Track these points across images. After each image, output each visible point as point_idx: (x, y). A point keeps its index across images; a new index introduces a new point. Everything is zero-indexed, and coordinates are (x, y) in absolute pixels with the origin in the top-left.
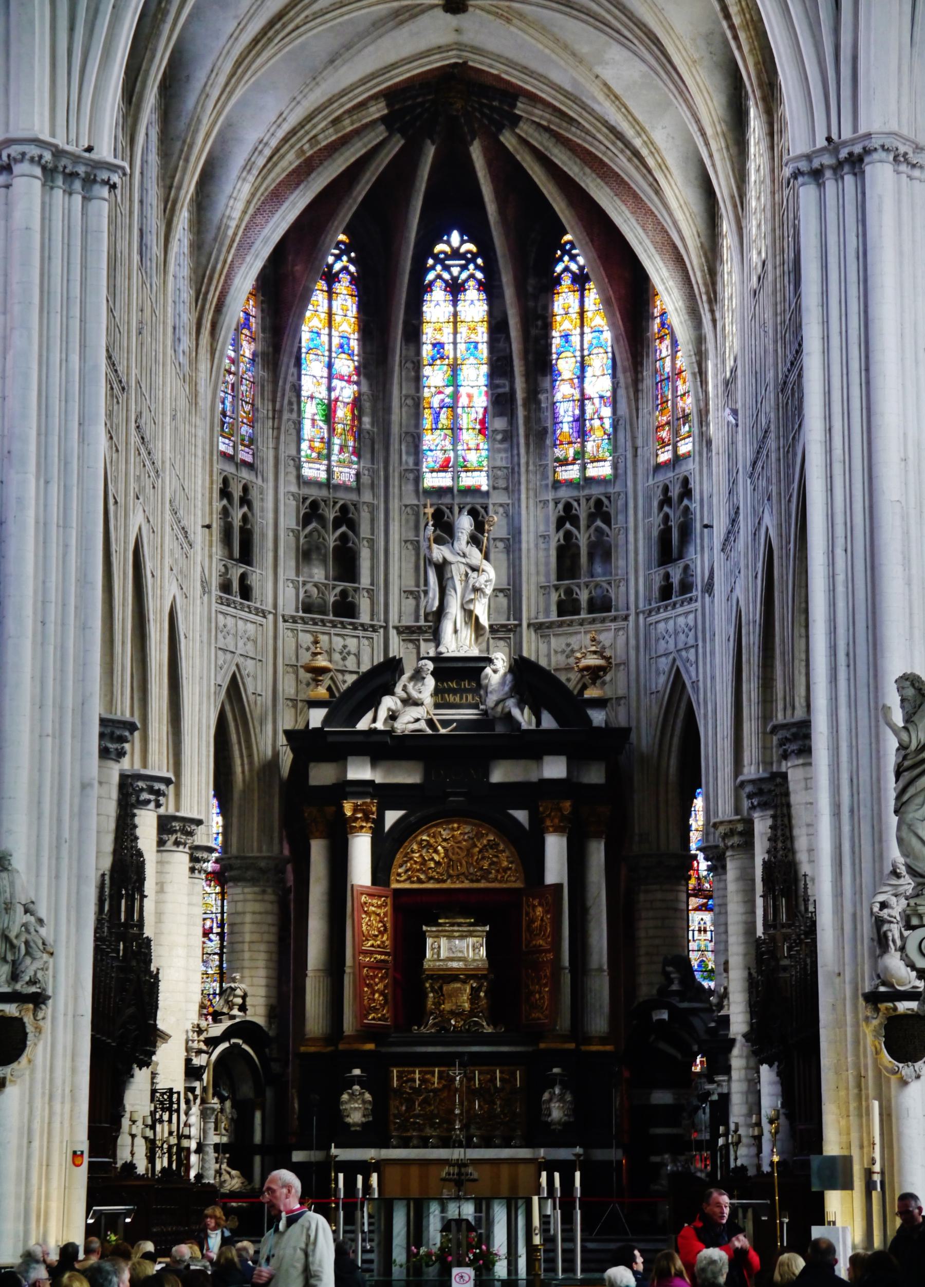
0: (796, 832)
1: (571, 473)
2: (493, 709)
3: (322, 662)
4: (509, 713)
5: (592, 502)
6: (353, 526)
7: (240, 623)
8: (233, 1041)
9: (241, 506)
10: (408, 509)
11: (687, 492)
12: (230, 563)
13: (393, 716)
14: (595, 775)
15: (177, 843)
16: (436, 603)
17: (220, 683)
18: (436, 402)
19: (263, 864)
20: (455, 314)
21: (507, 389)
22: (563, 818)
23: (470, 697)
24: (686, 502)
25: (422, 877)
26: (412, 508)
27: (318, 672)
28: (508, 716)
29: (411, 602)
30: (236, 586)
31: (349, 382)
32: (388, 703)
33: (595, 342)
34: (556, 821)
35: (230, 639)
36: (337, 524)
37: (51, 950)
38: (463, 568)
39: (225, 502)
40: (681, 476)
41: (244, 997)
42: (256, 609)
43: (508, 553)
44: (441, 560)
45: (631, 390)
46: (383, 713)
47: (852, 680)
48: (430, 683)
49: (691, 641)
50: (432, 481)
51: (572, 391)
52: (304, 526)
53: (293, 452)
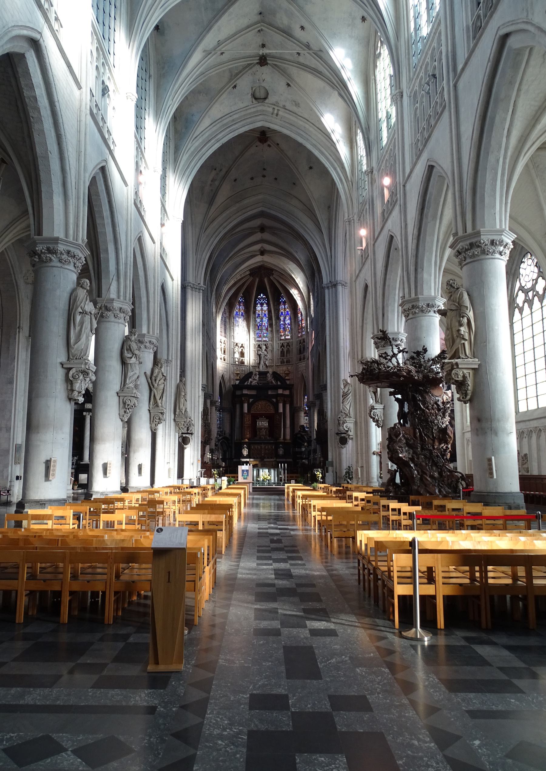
1: (283, 338)
6: (243, 347)
11: (304, 342)
14: (287, 392)
27: (238, 374)
28: (272, 382)
32: (250, 380)
36: (241, 347)
47: (334, 378)
48: (258, 376)
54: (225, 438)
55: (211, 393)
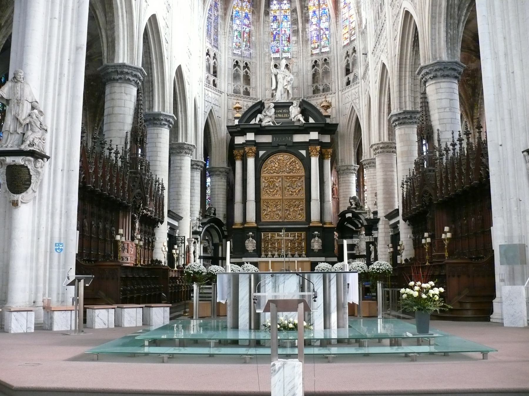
0: (432, 113)
2: (294, 118)
3: (238, 105)
4: (299, 119)
5: (323, 60)
7: (213, 94)
8: (211, 224)
9: (213, 59)
12: (210, 75)
13: (261, 120)
14: (327, 139)
15: (186, 153)
17: (206, 111)
18: (274, 33)
19: (221, 170)
20: (281, 7)
21: (296, 29)
22: (317, 151)
23: (286, 115)
24: (354, 54)
25: (272, 172)
28: (299, 120)
30: (212, 82)
31: (248, 27)
32: (259, 116)
33: (323, 12)
34: (315, 153)
35: (209, 98)
37: (45, 128)
38: (283, 75)
39: (208, 56)
40: (352, 47)
41: (215, 211)
42: (218, 90)
44: (276, 73)
45: (335, 24)
46: (258, 119)
49: (357, 97)
50: (273, 56)
51: (316, 27)
52: (234, 68)
53: (231, 46)
54: (217, 221)
55: (172, 114)
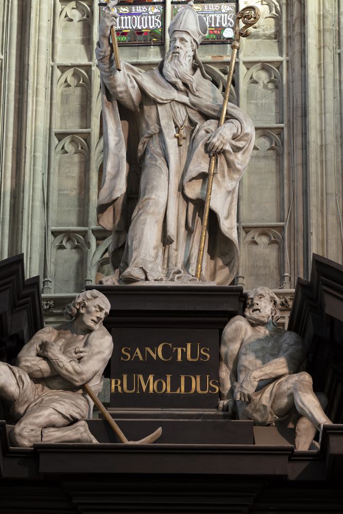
10: (69, 74)
16: (121, 188)
26: (76, 74)
29: (70, 255)
43: (279, 156)
44: (135, 93)
